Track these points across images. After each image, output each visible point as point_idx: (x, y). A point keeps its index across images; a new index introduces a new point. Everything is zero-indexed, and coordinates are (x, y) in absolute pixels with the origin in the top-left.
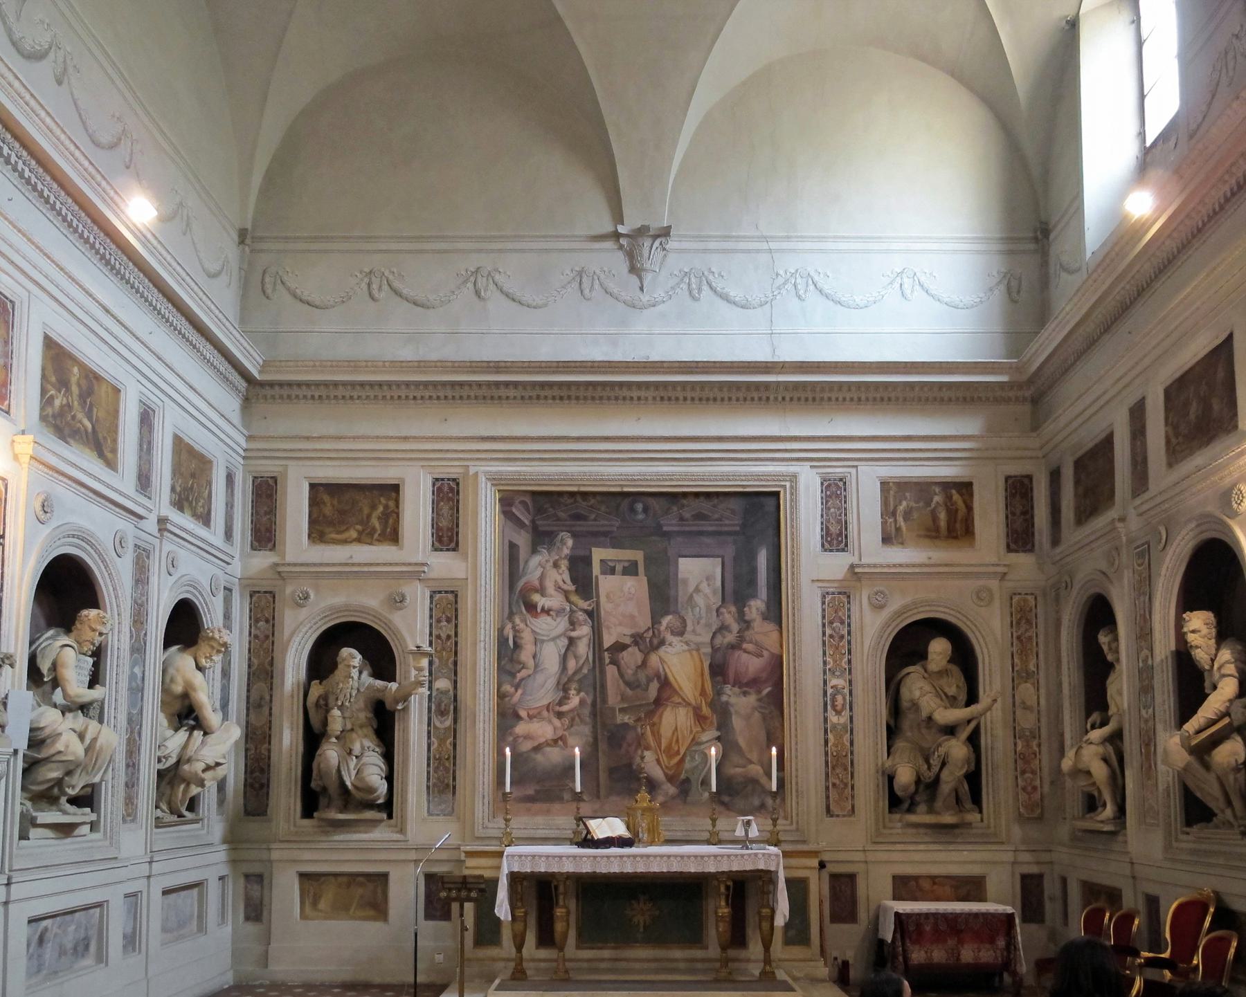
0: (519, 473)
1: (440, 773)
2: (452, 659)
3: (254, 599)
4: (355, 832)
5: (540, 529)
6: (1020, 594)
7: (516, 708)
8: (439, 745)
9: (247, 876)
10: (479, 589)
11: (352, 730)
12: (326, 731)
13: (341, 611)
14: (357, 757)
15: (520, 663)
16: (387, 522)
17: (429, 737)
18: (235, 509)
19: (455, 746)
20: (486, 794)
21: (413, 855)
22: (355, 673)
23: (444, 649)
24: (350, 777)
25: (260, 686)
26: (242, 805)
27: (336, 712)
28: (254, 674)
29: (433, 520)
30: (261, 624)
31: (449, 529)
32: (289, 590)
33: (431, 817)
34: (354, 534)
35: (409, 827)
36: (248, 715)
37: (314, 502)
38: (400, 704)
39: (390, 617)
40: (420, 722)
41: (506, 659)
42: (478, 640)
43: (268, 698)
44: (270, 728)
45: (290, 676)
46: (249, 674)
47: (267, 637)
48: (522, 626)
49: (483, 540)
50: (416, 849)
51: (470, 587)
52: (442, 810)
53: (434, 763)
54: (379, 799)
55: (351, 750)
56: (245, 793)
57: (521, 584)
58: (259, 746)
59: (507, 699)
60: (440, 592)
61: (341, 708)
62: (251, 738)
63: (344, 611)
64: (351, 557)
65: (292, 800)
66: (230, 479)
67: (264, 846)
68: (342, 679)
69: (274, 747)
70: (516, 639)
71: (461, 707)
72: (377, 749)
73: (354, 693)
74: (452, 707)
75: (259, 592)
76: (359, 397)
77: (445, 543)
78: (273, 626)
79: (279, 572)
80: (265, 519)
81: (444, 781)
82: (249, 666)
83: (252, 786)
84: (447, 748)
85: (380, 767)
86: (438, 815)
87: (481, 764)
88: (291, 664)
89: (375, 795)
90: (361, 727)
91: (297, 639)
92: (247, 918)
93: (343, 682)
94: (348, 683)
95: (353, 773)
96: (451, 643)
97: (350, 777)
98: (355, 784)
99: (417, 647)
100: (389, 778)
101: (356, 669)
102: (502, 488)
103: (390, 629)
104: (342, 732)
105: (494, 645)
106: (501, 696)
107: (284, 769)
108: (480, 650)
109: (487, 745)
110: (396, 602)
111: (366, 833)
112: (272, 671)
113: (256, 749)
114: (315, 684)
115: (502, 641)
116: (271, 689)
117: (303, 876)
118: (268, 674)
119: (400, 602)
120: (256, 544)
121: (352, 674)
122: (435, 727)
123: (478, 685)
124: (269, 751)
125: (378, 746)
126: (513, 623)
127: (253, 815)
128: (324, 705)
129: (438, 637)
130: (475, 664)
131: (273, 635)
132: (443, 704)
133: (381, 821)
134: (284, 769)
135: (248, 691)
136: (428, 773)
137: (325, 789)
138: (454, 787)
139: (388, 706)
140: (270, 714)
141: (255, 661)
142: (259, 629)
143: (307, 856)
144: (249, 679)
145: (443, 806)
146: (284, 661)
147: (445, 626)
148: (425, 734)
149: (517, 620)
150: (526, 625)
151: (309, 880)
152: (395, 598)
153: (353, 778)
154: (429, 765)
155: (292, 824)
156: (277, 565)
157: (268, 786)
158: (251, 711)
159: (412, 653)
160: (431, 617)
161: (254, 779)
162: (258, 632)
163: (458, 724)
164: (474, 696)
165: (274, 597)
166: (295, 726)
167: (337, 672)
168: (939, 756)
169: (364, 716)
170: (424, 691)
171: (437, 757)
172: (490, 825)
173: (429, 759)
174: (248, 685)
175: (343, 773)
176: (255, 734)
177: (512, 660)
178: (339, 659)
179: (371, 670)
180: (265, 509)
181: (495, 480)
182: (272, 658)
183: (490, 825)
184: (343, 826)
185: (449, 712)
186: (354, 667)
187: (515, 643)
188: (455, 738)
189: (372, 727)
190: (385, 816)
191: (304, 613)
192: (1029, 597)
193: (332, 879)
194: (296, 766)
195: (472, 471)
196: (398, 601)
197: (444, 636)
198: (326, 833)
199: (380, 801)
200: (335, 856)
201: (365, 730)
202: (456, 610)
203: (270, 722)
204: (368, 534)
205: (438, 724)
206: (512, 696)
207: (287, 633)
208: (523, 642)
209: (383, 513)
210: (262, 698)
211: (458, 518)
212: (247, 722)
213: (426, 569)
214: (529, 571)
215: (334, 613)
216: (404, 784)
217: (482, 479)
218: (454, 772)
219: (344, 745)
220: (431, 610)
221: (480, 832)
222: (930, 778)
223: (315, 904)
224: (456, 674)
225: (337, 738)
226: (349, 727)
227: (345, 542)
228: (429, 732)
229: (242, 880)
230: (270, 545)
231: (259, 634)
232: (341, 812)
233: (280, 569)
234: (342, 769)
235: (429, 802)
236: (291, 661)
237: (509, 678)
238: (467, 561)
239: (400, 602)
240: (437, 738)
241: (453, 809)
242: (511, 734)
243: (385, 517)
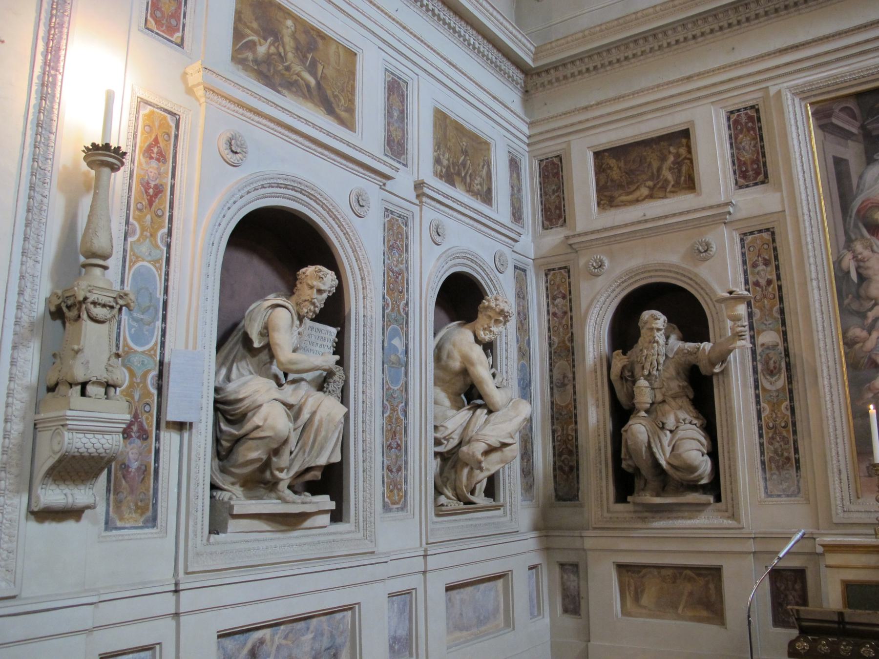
0: (835, 77)
1: (777, 445)
2: (777, 307)
3: (549, 277)
4: (677, 518)
5: (874, 133)
7: (873, 356)
8: (773, 411)
9: (562, 565)
10: (801, 219)
11: (664, 401)
12: (634, 404)
13: (638, 274)
14: (671, 431)
15: (871, 299)
16: (680, 171)
17: (758, 403)
18: (524, 193)
19: (793, 410)
20: (843, 467)
21: (751, 546)
22: (660, 337)
23: (765, 296)
24: (664, 455)
25: (562, 363)
26: (553, 491)
27: (642, 383)
28: (555, 352)
29: (733, 155)
30: (558, 301)
31: (753, 162)
32: (582, 262)
33: (770, 499)
34: (645, 191)
35: (743, 512)
36: (552, 395)
37: (600, 169)
38: (717, 367)
39: (696, 270)
40: (745, 385)
41: (850, 296)
42: (808, 279)
43: (570, 375)
44: (575, 408)
45: (591, 349)
46: (550, 353)
47: (565, 313)
48: (866, 253)
49: (798, 162)
50: (754, 538)
51: (788, 218)
52: (784, 490)
53: (767, 433)
54: (702, 478)
55: (663, 424)
56: (555, 477)
57: (856, 204)
58: (565, 427)
59: (857, 346)
60: (752, 233)
61: (648, 377)
62: (557, 419)
63: (642, 273)
64: (645, 215)
65: (604, 483)
66: (514, 164)
67: (577, 533)
68: (646, 345)
69: (581, 427)
70: (860, 271)
71: (795, 360)
72: (695, 421)
73: (661, 361)
74: (783, 365)
75: (553, 270)
76: (634, 55)
77: (752, 178)
78: (570, 300)
79: (570, 245)
80: (553, 197)
81: (782, 454)
82: (550, 345)
83: (561, 468)
84: (782, 413)
85: (699, 441)
86: (779, 496)
87: (831, 430)
88: (591, 337)
89: (696, 474)
90: (674, 397)
91: (594, 312)
92: (566, 611)
93: (647, 349)
94: (653, 348)
95: (668, 450)
96: (774, 289)
97: (664, 455)
98: (671, 462)
99: (731, 293)
100: (713, 454)
101: (661, 332)
102: (814, 100)
103: (696, 283)
104: (652, 404)
105: (831, 283)
106: (849, 343)
107: (592, 452)
108: (813, 290)
109: (836, 406)
110: (701, 252)
111: (690, 518)
112: (573, 347)
113: (563, 430)
114: (618, 355)
115: (841, 276)
116: (574, 366)
117: (622, 568)
118: (569, 351)
119: (705, 251)
120: (547, 223)
121: (657, 338)
122: (764, 389)
123: (815, 333)
124: (576, 431)
125: (697, 418)
126: (854, 252)
127: (565, 500)
128: (629, 376)
129: (757, 284)
130: (807, 307)
131: (571, 310)
132: (772, 362)
133: (709, 504)
134: (592, 452)
135: (551, 370)
136: (761, 445)
137: (637, 469)
138: (797, 461)
139: (704, 371)
140: (575, 393)
141: (555, 339)
142: (557, 306)
143: (625, 545)
144: (550, 358)
145: (785, 485)
146: (583, 334)
147: (763, 270)
148: (752, 399)
149: (859, 247)
150: (873, 251)
151: (628, 571)
152: (698, 249)
153: (668, 455)
154: (761, 436)
155: (605, 510)
156: (567, 238)
157: (578, 469)
158: (555, 391)
159: (724, 300)
160: (744, 263)
161: (563, 461)
162: (556, 310)
163: (794, 384)
164: (812, 346)
165: (569, 272)
166: (601, 403)
167: (641, 340)
169: (675, 385)
170: (746, 343)
171: (771, 425)
172: (853, 508)
173: (760, 428)
174: (551, 365)
175: (655, 450)
176: (561, 414)
177: (858, 297)
178: (640, 324)
179: (681, 335)
180: (554, 187)
181: (802, 94)
182: (572, 334)
183: (853, 508)
184: (663, 511)
185: (780, 369)
186: (659, 330)
187: (860, 276)
188: (792, 399)
189: (687, 397)
190: (711, 499)
191: (600, 282)
193: (655, 572)
194: (606, 447)
195: (773, 91)
196: (703, 252)
197: (763, 282)
198: (643, 519)
199: (704, 481)
200: (655, 546)
201: (679, 401)
202: (775, 249)
203: (575, 400)
204: (661, 188)
205: (768, 386)
206: (865, 340)
207: (584, 306)
208: (870, 272)
209: (674, 163)
210: (565, 376)
211: (762, 147)
212: (552, 403)
213: (731, 210)
214: (867, 185)
215: (632, 277)
216: (732, 459)
217: (787, 96)
218: (795, 442)
219: (656, 418)
220: (743, 254)
221: (839, 516)
223: (637, 599)
224: (784, 323)
225: (647, 411)
226: (659, 398)
227: (637, 201)
228: (757, 396)
229: (557, 569)
230: (561, 221)
231: (557, 311)
232: (658, 495)
233: (571, 242)
234: (653, 445)
235: (765, 479)
236: (591, 334)
237: (856, 320)
238: (781, 191)
239: (705, 251)
240: (769, 402)
241: (799, 489)
242: (869, 389)
243: (678, 164)
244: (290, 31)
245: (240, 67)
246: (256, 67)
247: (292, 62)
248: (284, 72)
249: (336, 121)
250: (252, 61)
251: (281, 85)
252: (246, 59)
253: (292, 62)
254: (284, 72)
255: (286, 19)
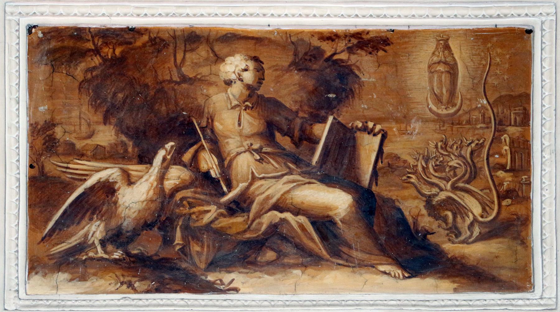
244: (237, 89)
245: (63, 276)
246: (117, 255)
247: (254, 179)
248: (224, 222)
249: (446, 284)
250: (103, 243)
251: (213, 265)
252: (81, 247)
253: (254, 179)
254: (224, 222)
255: (219, 59)
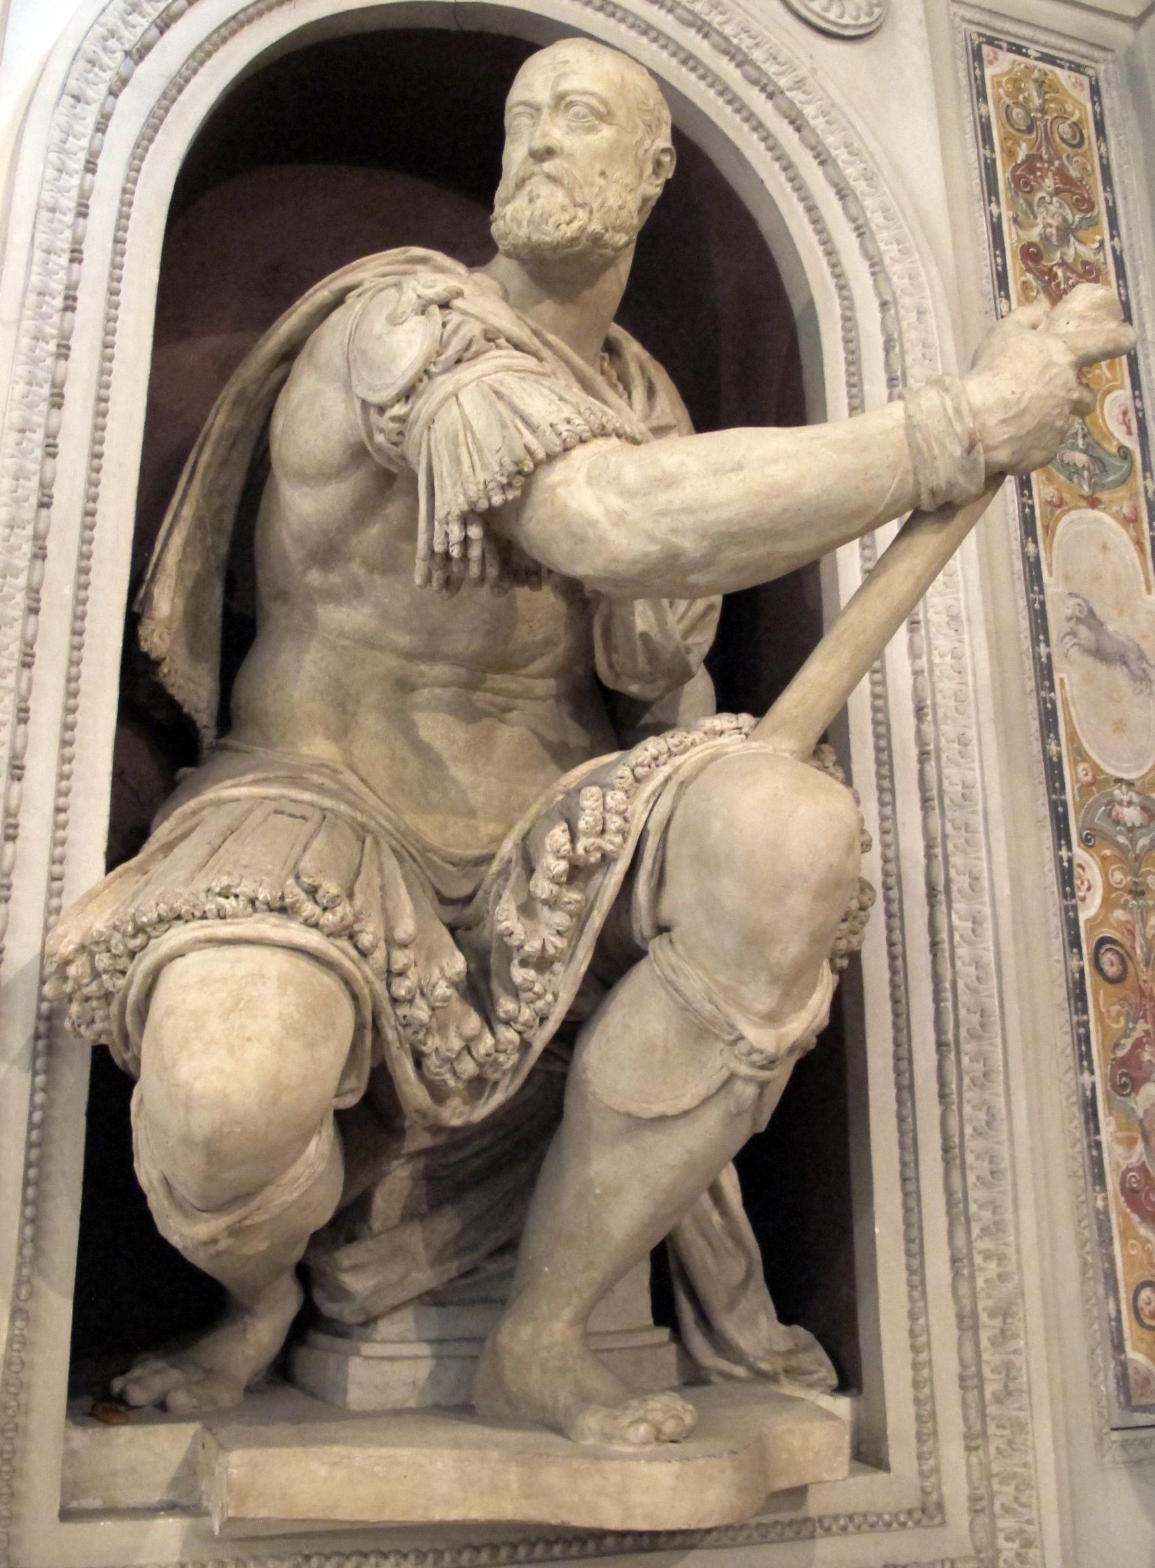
6: (1018, 50)
168: (578, 873)
192: (1063, 77)
222: (478, 1086)
